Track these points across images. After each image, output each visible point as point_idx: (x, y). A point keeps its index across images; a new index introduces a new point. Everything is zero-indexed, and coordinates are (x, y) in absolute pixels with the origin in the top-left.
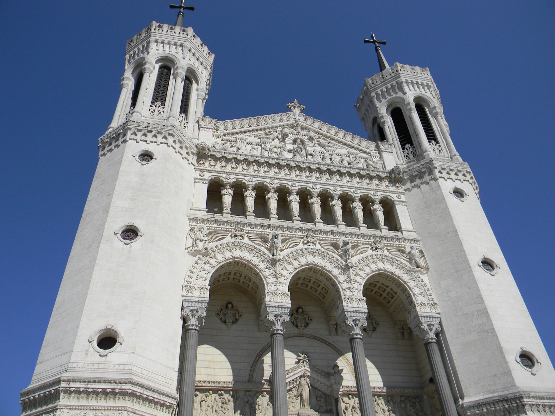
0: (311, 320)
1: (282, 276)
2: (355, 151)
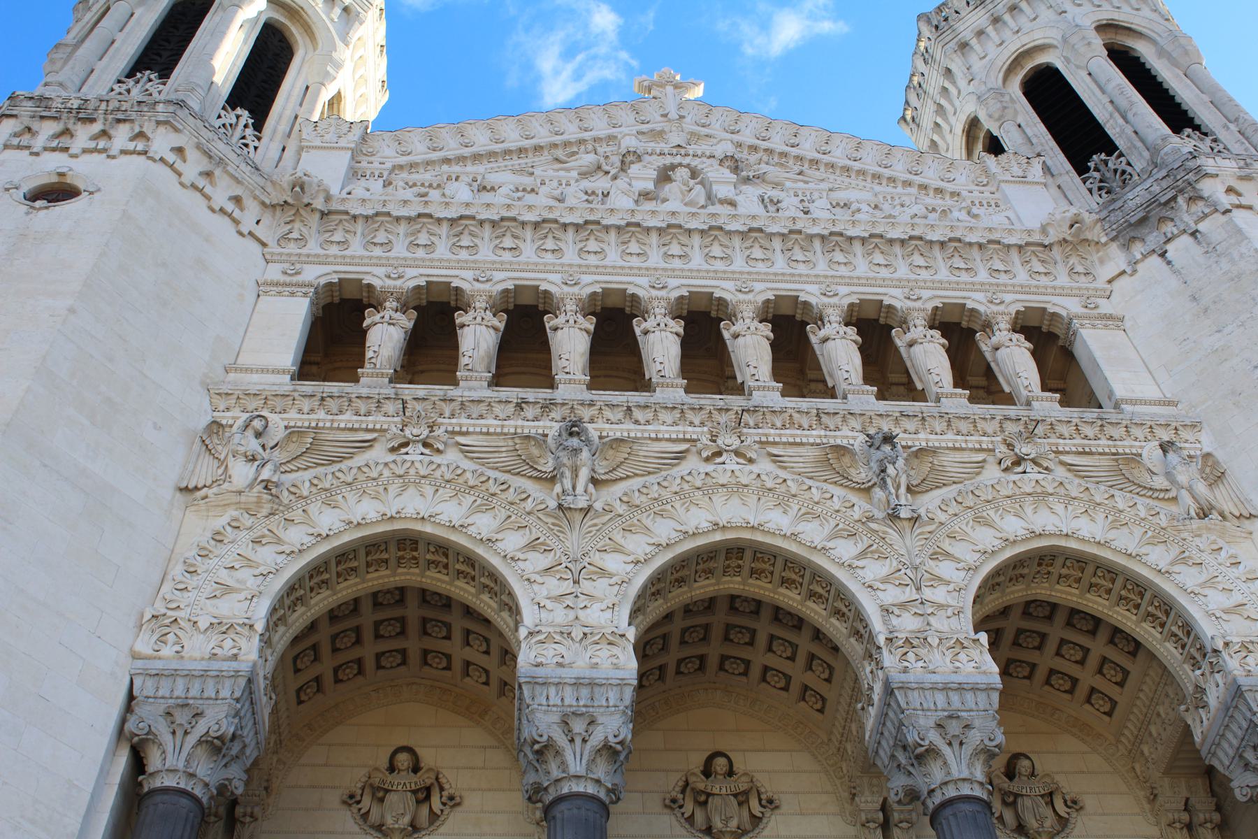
0: (770, 801)
1: (603, 572)
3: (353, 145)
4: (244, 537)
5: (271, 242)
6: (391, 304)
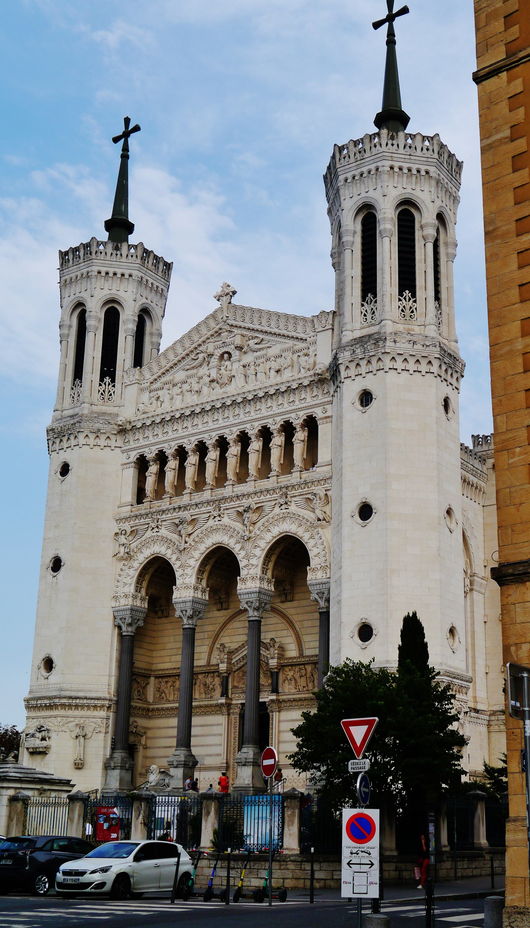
2: (290, 343)
3: (136, 381)
4: (127, 567)
5: (122, 445)
6: (151, 463)
